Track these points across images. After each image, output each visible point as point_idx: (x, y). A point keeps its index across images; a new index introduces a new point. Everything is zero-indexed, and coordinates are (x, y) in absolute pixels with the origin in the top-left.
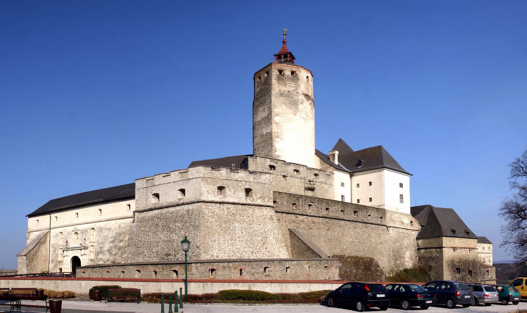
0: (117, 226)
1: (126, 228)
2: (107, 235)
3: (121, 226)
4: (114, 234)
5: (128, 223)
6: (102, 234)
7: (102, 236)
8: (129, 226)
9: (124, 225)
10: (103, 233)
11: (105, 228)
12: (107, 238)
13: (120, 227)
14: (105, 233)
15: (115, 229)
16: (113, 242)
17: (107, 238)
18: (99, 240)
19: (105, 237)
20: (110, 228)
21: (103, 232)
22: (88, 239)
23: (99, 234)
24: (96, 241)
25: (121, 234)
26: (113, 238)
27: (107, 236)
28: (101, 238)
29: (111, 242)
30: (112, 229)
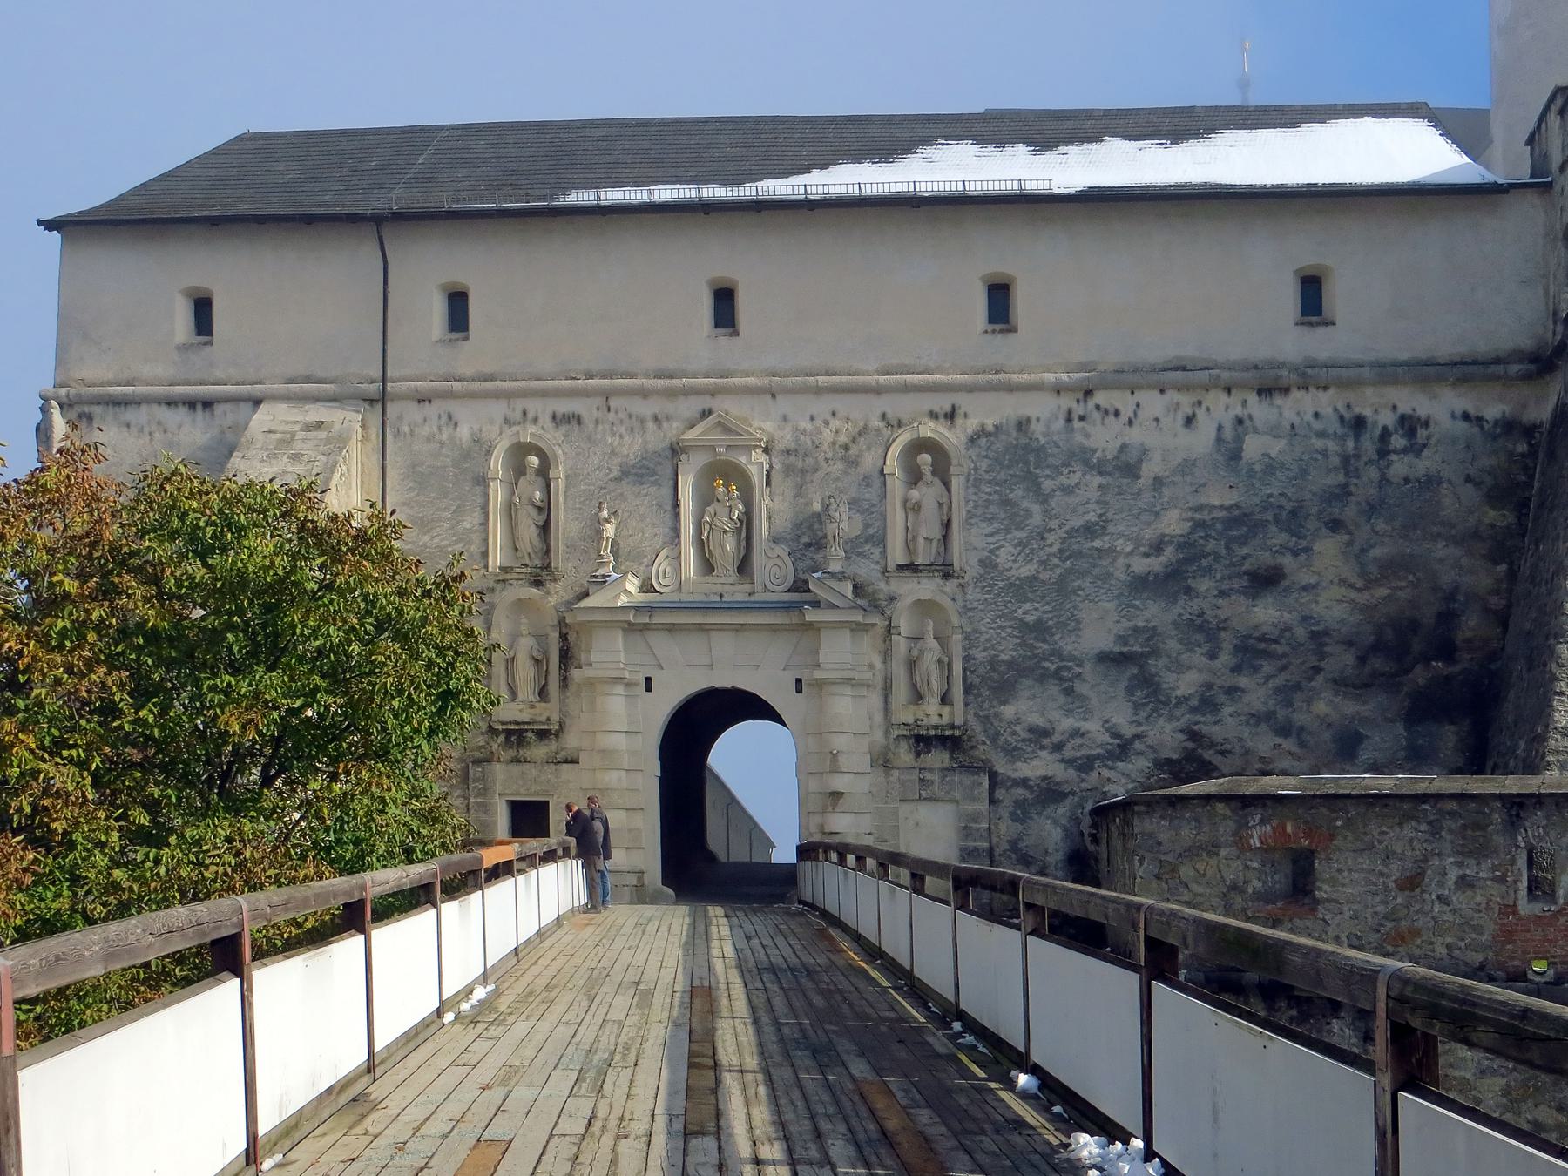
0: (1201, 441)
1: (1304, 472)
2: (1092, 517)
3: (1253, 447)
4: (1173, 523)
5: (1322, 435)
6: (1036, 509)
7: (1037, 519)
8: (1335, 461)
9: (1276, 447)
10: (1044, 499)
11: (1072, 455)
12: (1097, 543)
13: (1235, 455)
14: (1072, 500)
15: (1186, 467)
16: (1171, 582)
17: (1097, 543)
18: (1003, 558)
19: (1072, 533)
20: (1132, 456)
21: (1048, 485)
22: (881, 541)
23: (1006, 503)
24: (973, 570)
25: (1263, 524)
26: (1169, 553)
27: (1089, 531)
28: (1021, 544)
29: (1141, 584)
30: (1150, 469)
